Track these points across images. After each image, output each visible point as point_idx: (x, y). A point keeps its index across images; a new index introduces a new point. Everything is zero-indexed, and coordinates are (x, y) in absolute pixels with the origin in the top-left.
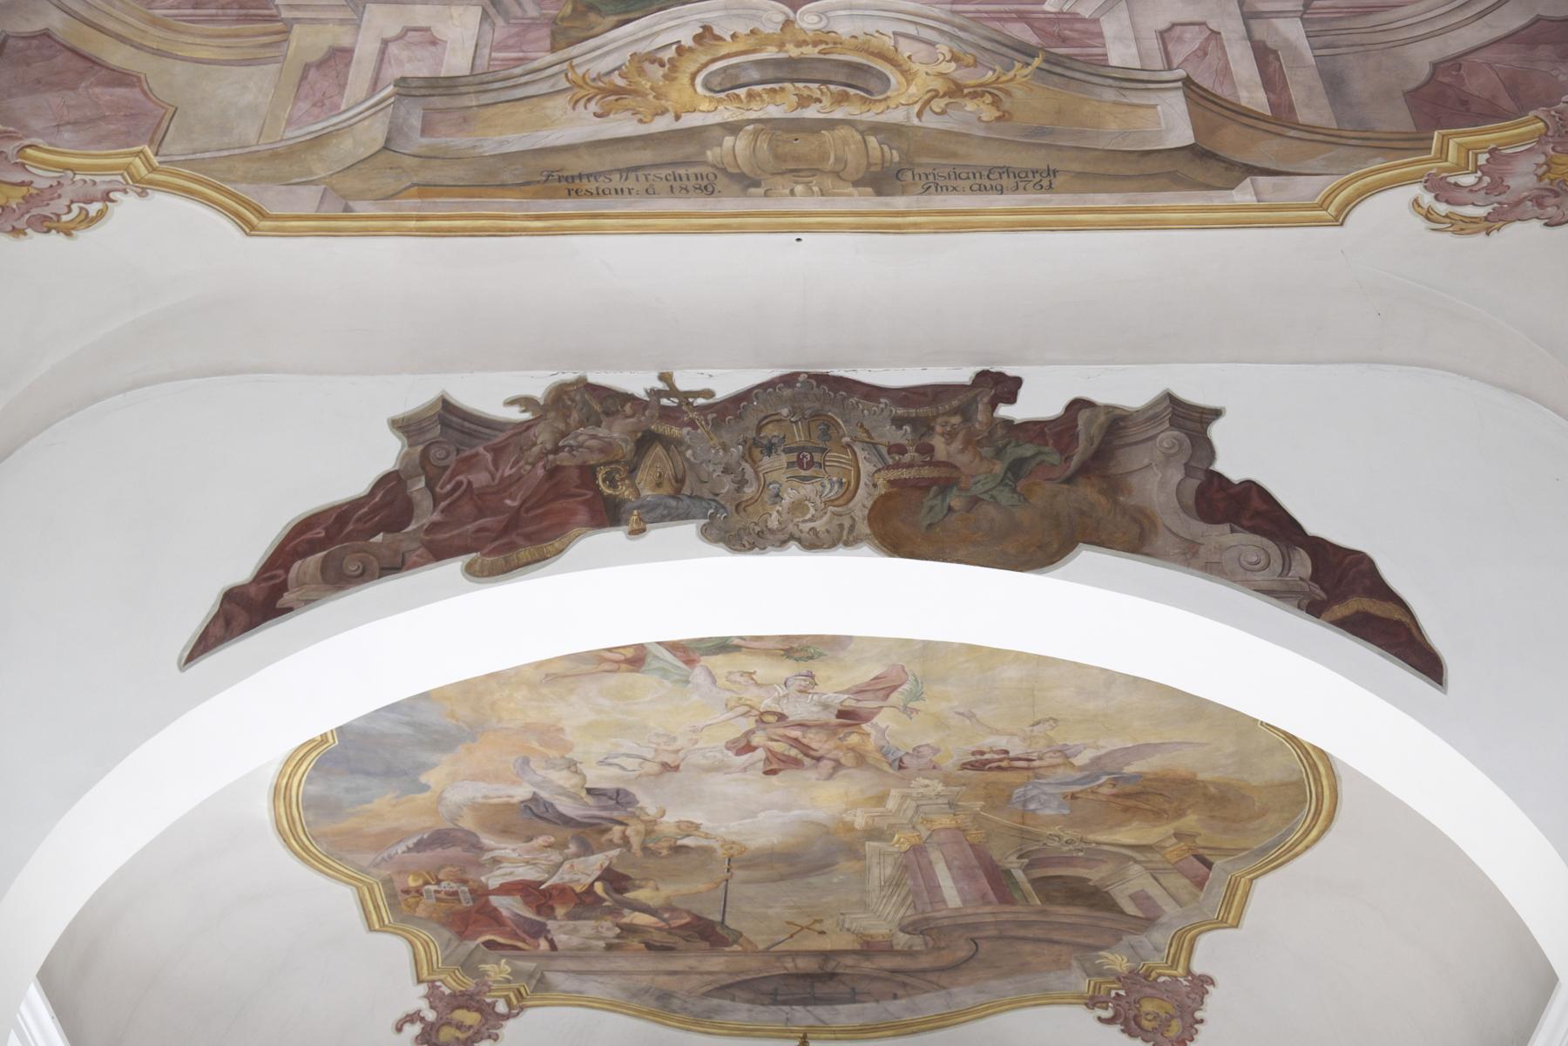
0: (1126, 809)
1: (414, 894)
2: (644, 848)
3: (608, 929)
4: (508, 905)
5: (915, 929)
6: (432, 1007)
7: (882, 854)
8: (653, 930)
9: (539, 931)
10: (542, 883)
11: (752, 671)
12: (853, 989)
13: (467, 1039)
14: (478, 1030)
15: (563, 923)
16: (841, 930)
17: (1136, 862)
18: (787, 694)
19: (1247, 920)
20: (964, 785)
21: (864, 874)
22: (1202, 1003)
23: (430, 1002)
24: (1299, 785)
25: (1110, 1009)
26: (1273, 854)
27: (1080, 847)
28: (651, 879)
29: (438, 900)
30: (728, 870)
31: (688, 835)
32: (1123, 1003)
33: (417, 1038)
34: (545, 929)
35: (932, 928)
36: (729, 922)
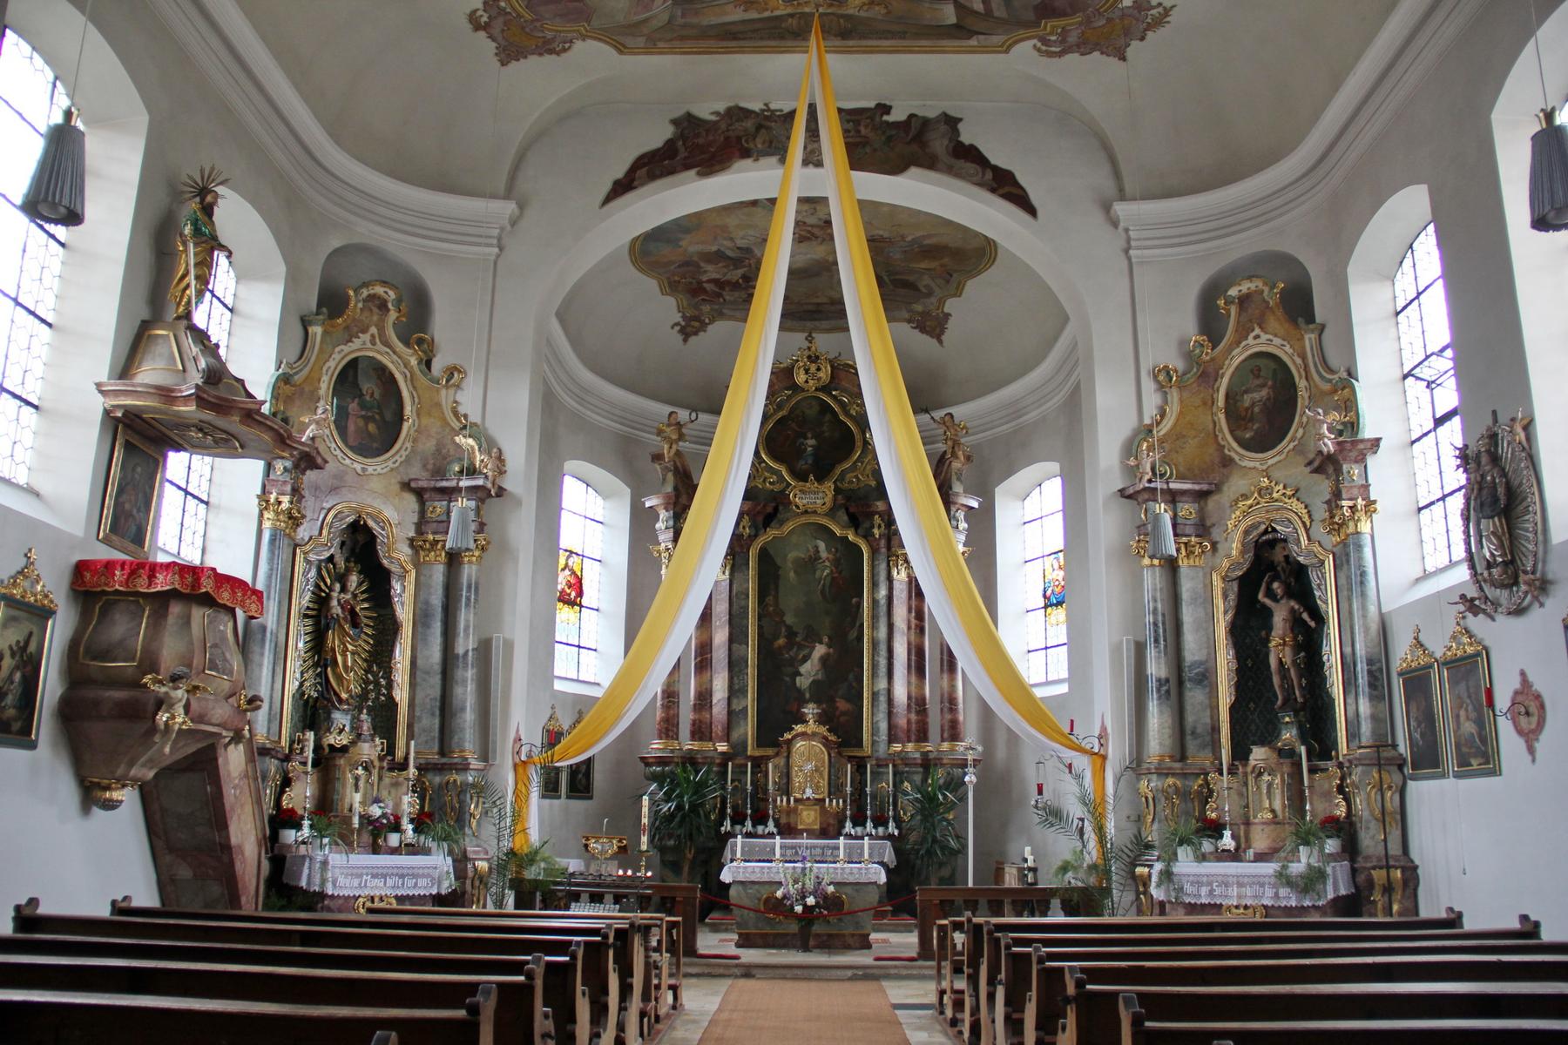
9: (719, 295)
19: (964, 295)
24: (984, 249)
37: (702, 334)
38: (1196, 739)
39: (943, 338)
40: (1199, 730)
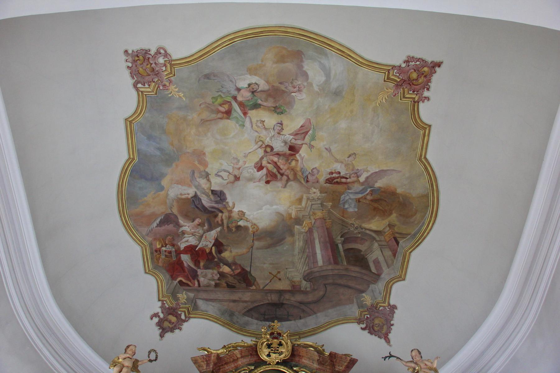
0: (375, 209)
1: (158, 252)
2: (228, 227)
3: (216, 275)
4: (186, 259)
5: (308, 279)
6: (162, 312)
7: (300, 233)
8: (229, 276)
9: (194, 275)
10: (197, 246)
11: (264, 120)
12: (288, 312)
13: (172, 327)
14: (176, 325)
15: (202, 271)
16: (286, 278)
17: (377, 241)
18: (274, 135)
20: (326, 192)
21: (293, 243)
22: (393, 317)
23: (162, 310)
24: (427, 196)
25: (365, 324)
26: (418, 236)
27: (359, 231)
28: (229, 246)
29: (166, 256)
30: (253, 242)
31: (241, 219)
32: (369, 321)
33: (157, 323)
34: (197, 274)
35: (312, 278)
36: (252, 272)
37: (177, 331)
39: (390, 336)
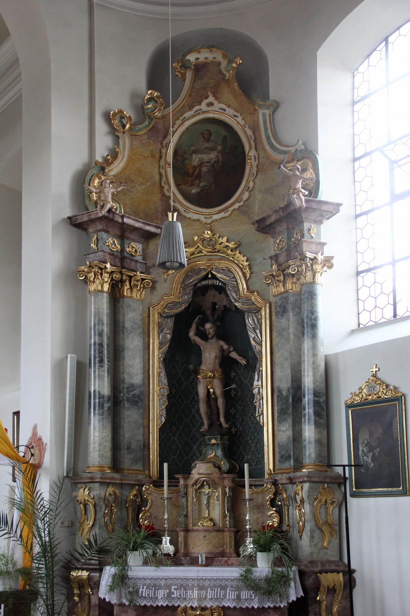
38: (130, 453)
40: (133, 446)
